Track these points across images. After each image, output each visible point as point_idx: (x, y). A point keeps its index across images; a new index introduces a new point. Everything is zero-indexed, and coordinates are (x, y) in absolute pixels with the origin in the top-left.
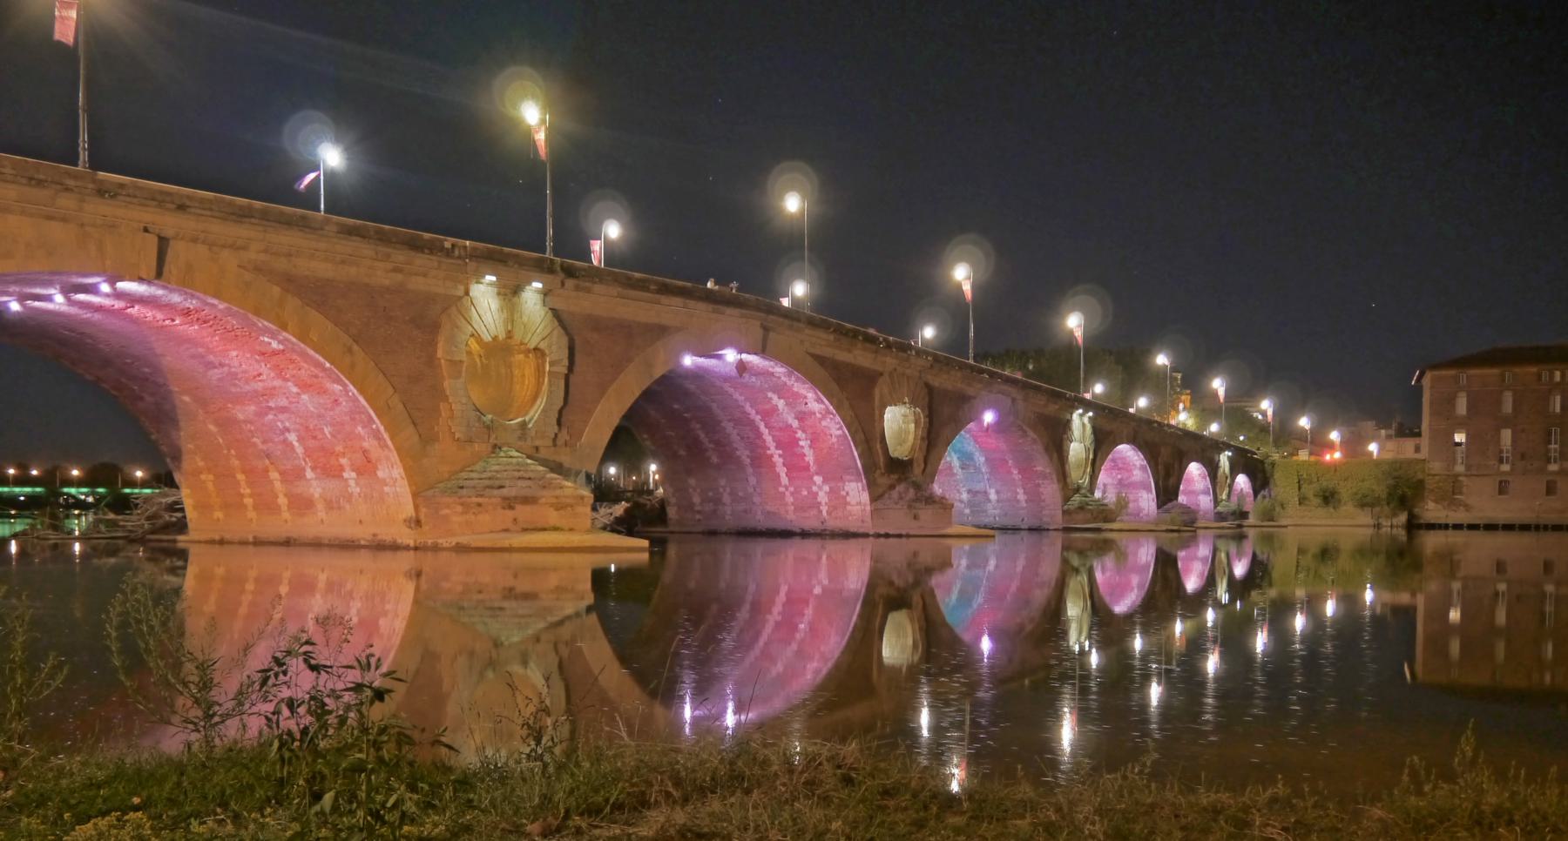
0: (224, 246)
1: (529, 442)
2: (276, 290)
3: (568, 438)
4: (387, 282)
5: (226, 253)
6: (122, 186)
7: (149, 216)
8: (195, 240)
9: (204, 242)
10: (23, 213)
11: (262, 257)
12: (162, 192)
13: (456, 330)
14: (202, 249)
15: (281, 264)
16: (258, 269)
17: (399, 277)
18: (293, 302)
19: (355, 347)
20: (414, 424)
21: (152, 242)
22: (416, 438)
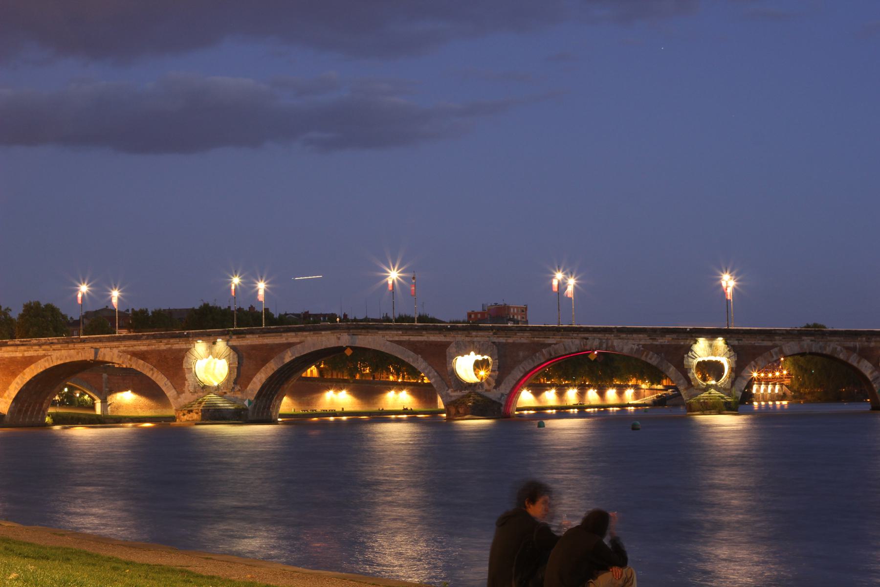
0: (113, 347)
1: (220, 391)
2: (129, 356)
3: (240, 388)
4: (165, 348)
5: (115, 349)
6: (86, 338)
7: (90, 345)
8: (105, 348)
9: (108, 347)
10: (64, 349)
11: (125, 348)
12: (96, 338)
13: (189, 359)
14: (108, 349)
15: (131, 349)
16: (124, 352)
17: (170, 346)
18: (134, 359)
19: (154, 369)
20: (175, 388)
21: (93, 350)
22: (175, 393)
